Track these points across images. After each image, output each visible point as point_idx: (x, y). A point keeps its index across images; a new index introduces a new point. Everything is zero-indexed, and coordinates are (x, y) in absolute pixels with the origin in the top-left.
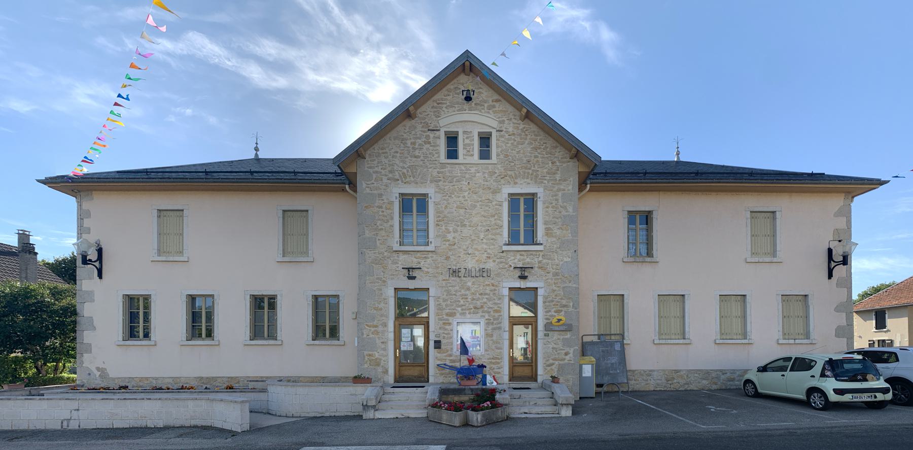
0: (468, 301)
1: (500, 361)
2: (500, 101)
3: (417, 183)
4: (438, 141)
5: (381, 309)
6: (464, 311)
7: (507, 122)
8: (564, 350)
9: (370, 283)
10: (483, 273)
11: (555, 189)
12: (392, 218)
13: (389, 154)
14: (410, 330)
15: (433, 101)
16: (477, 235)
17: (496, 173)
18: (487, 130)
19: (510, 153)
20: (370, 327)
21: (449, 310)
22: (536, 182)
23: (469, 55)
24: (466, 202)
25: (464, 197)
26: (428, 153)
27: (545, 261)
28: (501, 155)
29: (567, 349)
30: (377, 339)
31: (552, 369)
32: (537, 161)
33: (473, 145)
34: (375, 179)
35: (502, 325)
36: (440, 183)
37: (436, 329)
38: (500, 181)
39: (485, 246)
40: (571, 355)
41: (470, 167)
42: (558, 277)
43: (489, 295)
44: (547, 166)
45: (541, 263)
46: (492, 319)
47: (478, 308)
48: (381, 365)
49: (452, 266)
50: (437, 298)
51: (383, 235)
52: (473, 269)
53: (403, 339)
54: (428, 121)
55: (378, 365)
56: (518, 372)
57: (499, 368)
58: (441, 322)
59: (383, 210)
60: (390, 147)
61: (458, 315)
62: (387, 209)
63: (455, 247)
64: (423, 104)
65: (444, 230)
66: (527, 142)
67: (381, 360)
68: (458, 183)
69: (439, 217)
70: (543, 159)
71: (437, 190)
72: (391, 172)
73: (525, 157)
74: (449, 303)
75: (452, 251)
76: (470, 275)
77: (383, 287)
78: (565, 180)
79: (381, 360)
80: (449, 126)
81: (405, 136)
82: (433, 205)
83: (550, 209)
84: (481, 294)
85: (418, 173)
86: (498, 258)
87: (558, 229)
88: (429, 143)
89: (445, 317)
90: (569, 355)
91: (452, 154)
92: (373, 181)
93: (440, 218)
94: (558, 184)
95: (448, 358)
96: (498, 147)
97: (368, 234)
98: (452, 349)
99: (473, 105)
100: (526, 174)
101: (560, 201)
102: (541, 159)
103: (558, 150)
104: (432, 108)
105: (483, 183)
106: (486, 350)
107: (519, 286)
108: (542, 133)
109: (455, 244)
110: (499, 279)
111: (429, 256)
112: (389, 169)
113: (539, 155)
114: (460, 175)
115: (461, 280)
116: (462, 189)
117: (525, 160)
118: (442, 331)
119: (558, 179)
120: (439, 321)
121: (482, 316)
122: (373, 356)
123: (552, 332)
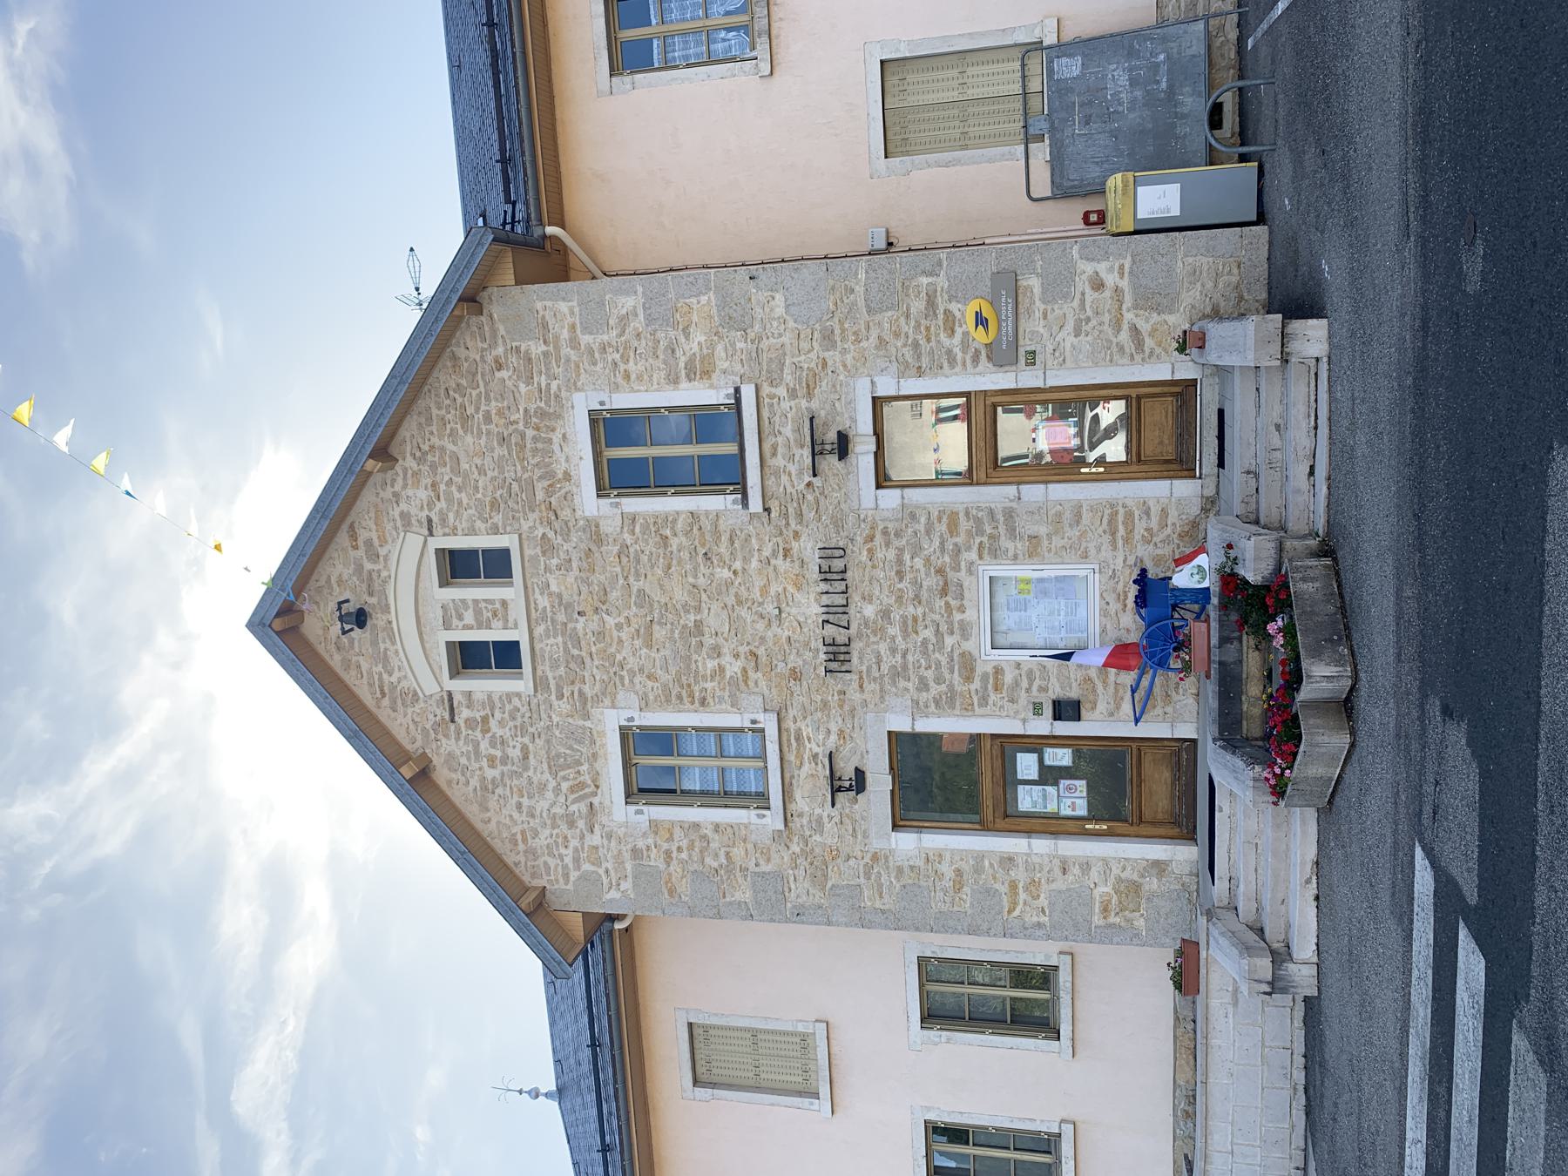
0: (924, 614)
1: (1121, 511)
2: (352, 526)
3: (595, 756)
4: (477, 696)
5: (959, 873)
6: (956, 625)
7: (403, 506)
8: (1083, 294)
9: (881, 897)
10: (833, 571)
12: (696, 826)
13: (525, 826)
14: (1020, 788)
16: (724, 589)
17: (544, 534)
18: (431, 561)
19: (484, 496)
20: (1014, 904)
21: (952, 671)
22: (559, 416)
25: (619, 627)
26: (511, 724)
27: (788, 378)
28: (495, 520)
29: (1082, 284)
30: (1054, 886)
31: (1154, 331)
32: (500, 413)
33: (476, 602)
34: (593, 864)
35: (998, 508)
36: (587, 689)
38: (566, 523)
39: (754, 563)
40: (1102, 267)
41: (537, 611)
42: (837, 331)
43: (901, 550)
45: (794, 390)
46: (978, 540)
47: (946, 584)
48: (1135, 877)
49: (818, 661)
50: (918, 709)
51: (743, 853)
52: (825, 600)
53: (1052, 807)
54: (431, 723)
55: (1136, 888)
56: (1161, 443)
57: (1147, 513)
58: (993, 697)
59: (674, 849)
60: (507, 821)
61: (968, 646)
62: (671, 839)
63: (761, 652)
64: (387, 733)
65: (713, 684)
66: (450, 447)
67: (1119, 880)
68: (583, 643)
69: (680, 697)
70: (492, 395)
71: (607, 702)
72: (572, 824)
73: (493, 450)
74: (930, 672)
75: (775, 662)
77: (891, 864)
78: (545, 326)
79: (1119, 880)
80: (435, 667)
81: (474, 782)
82: (649, 715)
83: (631, 366)
85: (568, 752)
86: (788, 524)
87: (687, 338)
88: (485, 720)
89: (976, 684)
90: (1103, 275)
91: (506, 656)
92: (601, 871)
93: (684, 694)
94: (557, 348)
96: (472, 532)
97: (744, 894)
99: (373, 600)
100: (540, 446)
101: (605, 337)
102: (493, 403)
103: (461, 352)
104: (395, 711)
105: (576, 572)
106: (1085, 556)
107: (871, 458)
108: (421, 403)
110: (851, 519)
111: (792, 727)
112: (564, 827)
113: (483, 408)
114: (560, 639)
115: (860, 635)
116: (599, 633)
117: (500, 451)
119: (544, 348)
120: (990, 702)
121: (970, 572)
122: (1109, 901)
123: (1021, 342)
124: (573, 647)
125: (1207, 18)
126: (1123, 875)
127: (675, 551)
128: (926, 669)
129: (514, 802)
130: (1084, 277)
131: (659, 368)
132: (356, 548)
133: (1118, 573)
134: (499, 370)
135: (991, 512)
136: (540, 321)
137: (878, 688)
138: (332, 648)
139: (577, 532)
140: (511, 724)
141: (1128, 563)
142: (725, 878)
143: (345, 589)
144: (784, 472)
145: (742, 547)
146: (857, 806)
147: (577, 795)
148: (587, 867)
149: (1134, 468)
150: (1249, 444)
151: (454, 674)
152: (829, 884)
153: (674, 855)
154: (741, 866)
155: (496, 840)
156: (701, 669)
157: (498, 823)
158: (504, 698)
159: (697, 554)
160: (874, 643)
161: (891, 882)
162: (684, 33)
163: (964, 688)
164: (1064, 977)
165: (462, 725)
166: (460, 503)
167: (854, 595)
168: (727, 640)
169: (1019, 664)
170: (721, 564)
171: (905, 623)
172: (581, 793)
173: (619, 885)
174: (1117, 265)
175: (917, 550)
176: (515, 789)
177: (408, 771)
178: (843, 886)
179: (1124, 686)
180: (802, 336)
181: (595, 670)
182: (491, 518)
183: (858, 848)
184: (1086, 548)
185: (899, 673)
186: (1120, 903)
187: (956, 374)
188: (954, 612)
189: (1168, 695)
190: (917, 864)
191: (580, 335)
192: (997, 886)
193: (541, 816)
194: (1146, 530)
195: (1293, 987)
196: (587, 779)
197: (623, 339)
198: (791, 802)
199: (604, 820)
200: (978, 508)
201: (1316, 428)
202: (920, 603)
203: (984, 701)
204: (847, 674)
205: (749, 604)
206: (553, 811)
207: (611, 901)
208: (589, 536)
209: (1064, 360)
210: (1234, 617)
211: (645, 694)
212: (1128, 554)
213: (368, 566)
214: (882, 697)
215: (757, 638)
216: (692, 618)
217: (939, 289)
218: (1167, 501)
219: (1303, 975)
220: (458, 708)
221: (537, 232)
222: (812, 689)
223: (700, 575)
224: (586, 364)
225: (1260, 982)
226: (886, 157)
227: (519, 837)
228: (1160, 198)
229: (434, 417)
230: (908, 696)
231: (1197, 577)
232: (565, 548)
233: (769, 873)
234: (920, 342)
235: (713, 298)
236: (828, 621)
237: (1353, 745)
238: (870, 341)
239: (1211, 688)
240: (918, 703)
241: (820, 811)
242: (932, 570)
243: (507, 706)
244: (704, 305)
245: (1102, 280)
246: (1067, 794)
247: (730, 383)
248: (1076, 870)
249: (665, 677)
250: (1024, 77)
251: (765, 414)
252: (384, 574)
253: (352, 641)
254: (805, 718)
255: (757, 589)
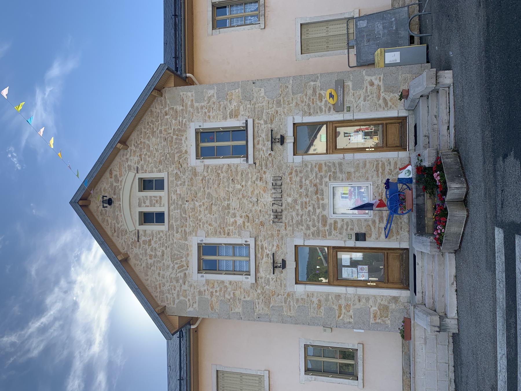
1: (380, 163)
2: (111, 170)
3: (188, 255)
4: (148, 232)
5: (320, 301)
6: (321, 205)
7: (129, 163)
8: (367, 87)
9: (290, 311)
10: (278, 184)
11: (192, 111)
12: (223, 282)
13: (161, 282)
14: (343, 269)
15: (113, 236)
16: (238, 192)
17: (176, 172)
18: (137, 181)
19: (157, 159)
21: (319, 223)
22: (185, 131)
23: (73, 201)
24: (205, 204)
25: (200, 206)
26: (159, 242)
28: (160, 168)
29: (366, 84)
30: (355, 307)
31: (391, 99)
32: (165, 130)
33: (151, 197)
34: (184, 297)
35: (336, 162)
36: (187, 230)
37: (342, 238)
38: (184, 168)
39: (249, 183)
40: (373, 78)
41: (172, 200)
43: (301, 178)
44: (169, 120)
45: (266, 121)
46: (329, 174)
47: (317, 190)
48: (386, 303)
49: (270, 219)
51: (239, 293)
52: (274, 196)
57: (390, 163)
58: (333, 232)
59: (214, 291)
60: (154, 280)
61: (325, 213)
62: (213, 287)
63: (250, 215)
65: (233, 227)
66: (147, 142)
67: (380, 304)
68: (187, 212)
69: (220, 232)
71: (194, 234)
72: (177, 281)
73: (161, 143)
76: (279, 199)
78: (183, 100)
79: (380, 304)
80: (135, 222)
81: (144, 265)
83: (211, 114)
84: (301, 186)
85: (178, 253)
86: (262, 169)
87: (231, 104)
89: (327, 228)
90: (374, 81)
91: (159, 218)
92: (187, 300)
95: (377, 225)
96: (152, 172)
97: (239, 309)
98: (366, 220)
99: (115, 197)
100: (177, 141)
101: (203, 104)
102: (163, 127)
103: (154, 110)
104: (118, 237)
105: (186, 186)
106: (367, 179)
107: (292, 144)
108: (139, 127)
109: (247, 216)
110: (284, 167)
112: (175, 282)
113: (160, 128)
114: (179, 211)
115: (286, 209)
116: (193, 209)
118: (344, 231)
119: (182, 108)
120: (333, 234)
121: (326, 185)
122: (377, 313)
124: (184, 214)
125: (408, 6)
126: (382, 303)
127: (222, 179)
128: (309, 221)
129: (157, 272)
130: (367, 81)
131: (220, 114)
132: (111, 178)
133: (379, 186)
134: (166, 115)
135: (334, 164)
136: (181, 98)
137: (292, 229)
138: (99, 214)
139: (188, 172)
140: (159, 242)
141: (383, 182)
142: (232, 303)
143: (106, 192)
144: (261, 150)
145: (245, 177)
146: (282, 275)
147: (180, 270)
148: (182, 298)
149: (385, 148)
150: (426, 126)
151: (141, 224)
152: (271, 306)
153: (214, 293)
154: (238, 298)
155: (150, 287)
156: (228, 222)
157: (151, 280)
158: (157, 233)
159: (229, 180)
160: (291, 212)
161: (294, 305)
162: (237, 18)
163: (323, 229)
164: (360, 354)
165: (142, 243)
166: (149, 161)
167: (284, 194)
168: (238, 211)
169: (343, 220)
170: (238, 183)
171: (302, 204)
172: (182, 269)
173: (193, 305)
174: (378, 77)
175: (307, 177)
176: (158, 267)
177: (120, 258)
178: (276, 306)
179: (382, 228)
180: (270, 103)
181: (191, 223)
182: (159, 167)
183: (282, 291)
184: (368, 176)
185: (300, 223)
186: (381, 314)
187: (322, 115)
188: (320, 200)
189: (398, 231)
190: (304, 298)
191: (194, 103)
192: (334, 306)
193: (167, 278)
194: (389, 170)
195: (448, 329)
196: (184, 263)
197: (209, 104)
198: (258, 273)
199: (189, 280)
200: (329, 162)
201: (449, 112)
202: (308, 197)
203: (330, 234)
204: (281, 223)
205: (247, 197)
206: (171, 276)
207: (190, 311)
208: (192, 173)
209: (360, 110)
210: (421, 187)
211: (208, 231)
212: (383, 178)
213: (115, 184)
214: (293, 232)
215: (249, 210)
216: (226, 203)
217: (317, 86)
218: (396, 159)
219: (452, 324)
220: (141, 236)
221: (184, 75)
222: (268, 229)
223: (230, 187)
224: (195, 113)
225: (435, 326)
226: (301, 54)
227: (158, 286)
228: (393, 56)
229: (143, 132)
230: (302, 232)
231: (407, 174)
232: (183, 177)
233: (249, 301)
234: (310, 104)
235: (240, 90)
236: (275, 204)
237: (468, 216)
238: (293, 104)
239: (414, 215)
240: (306, 234)
241: (269, 276)
242: (313, 185)
243: (158, 235)
244: (237, 93)
245: (373, 82)
246: (361, 271)
247: (244, 119)
248: (364, 300)
249: (215, 225)
250: (348, 28)
251: (256, 129)
252: (120, 187)
253: (106, 212)
254: (265, 240)
255: (250, 192)
